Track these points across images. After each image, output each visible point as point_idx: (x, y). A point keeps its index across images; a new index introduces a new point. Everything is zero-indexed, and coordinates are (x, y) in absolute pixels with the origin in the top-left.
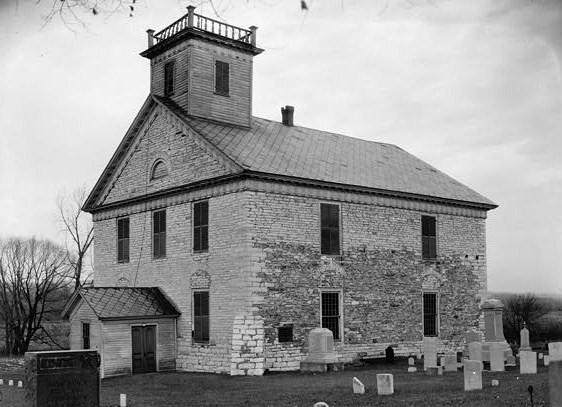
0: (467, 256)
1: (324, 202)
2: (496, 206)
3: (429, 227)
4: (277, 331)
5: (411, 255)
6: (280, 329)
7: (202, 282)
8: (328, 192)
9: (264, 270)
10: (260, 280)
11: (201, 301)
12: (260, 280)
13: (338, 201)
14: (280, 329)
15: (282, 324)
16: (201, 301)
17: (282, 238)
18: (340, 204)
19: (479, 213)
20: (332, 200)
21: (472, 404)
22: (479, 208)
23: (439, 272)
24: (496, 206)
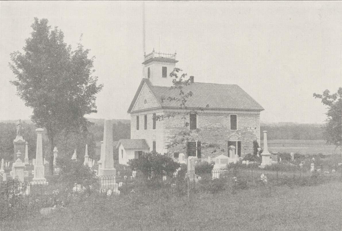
0: (251, 128)
1: (232, 114)
2: (178, 61)
3: (234, 119)
4: (173, 154)
5: (226, 129)
6: (175, 153)
7: (154, 138)
8: (176, 110)
9: (169, 136)
10: (167, 138)
11: (154, 143)
12: (167, 138)
13: (236, 114)
14: (175, 153)
15: (175, 152)
16: (154, 143)
17: (175, 125)
18: (237, 115)
19: (256, 113)
20: (232, 114)
21: (234, 228)
22: (258, 111)
23: (238, 134)
24: (178, 61)
